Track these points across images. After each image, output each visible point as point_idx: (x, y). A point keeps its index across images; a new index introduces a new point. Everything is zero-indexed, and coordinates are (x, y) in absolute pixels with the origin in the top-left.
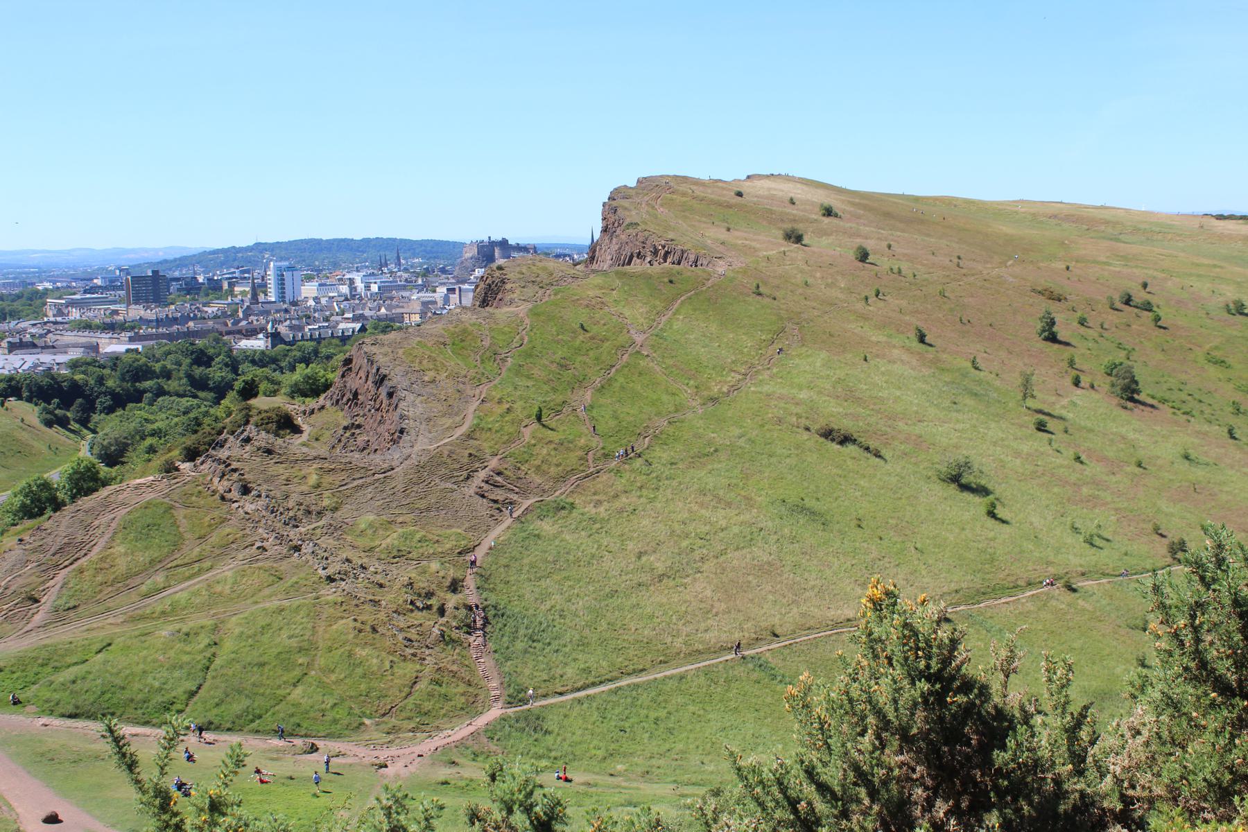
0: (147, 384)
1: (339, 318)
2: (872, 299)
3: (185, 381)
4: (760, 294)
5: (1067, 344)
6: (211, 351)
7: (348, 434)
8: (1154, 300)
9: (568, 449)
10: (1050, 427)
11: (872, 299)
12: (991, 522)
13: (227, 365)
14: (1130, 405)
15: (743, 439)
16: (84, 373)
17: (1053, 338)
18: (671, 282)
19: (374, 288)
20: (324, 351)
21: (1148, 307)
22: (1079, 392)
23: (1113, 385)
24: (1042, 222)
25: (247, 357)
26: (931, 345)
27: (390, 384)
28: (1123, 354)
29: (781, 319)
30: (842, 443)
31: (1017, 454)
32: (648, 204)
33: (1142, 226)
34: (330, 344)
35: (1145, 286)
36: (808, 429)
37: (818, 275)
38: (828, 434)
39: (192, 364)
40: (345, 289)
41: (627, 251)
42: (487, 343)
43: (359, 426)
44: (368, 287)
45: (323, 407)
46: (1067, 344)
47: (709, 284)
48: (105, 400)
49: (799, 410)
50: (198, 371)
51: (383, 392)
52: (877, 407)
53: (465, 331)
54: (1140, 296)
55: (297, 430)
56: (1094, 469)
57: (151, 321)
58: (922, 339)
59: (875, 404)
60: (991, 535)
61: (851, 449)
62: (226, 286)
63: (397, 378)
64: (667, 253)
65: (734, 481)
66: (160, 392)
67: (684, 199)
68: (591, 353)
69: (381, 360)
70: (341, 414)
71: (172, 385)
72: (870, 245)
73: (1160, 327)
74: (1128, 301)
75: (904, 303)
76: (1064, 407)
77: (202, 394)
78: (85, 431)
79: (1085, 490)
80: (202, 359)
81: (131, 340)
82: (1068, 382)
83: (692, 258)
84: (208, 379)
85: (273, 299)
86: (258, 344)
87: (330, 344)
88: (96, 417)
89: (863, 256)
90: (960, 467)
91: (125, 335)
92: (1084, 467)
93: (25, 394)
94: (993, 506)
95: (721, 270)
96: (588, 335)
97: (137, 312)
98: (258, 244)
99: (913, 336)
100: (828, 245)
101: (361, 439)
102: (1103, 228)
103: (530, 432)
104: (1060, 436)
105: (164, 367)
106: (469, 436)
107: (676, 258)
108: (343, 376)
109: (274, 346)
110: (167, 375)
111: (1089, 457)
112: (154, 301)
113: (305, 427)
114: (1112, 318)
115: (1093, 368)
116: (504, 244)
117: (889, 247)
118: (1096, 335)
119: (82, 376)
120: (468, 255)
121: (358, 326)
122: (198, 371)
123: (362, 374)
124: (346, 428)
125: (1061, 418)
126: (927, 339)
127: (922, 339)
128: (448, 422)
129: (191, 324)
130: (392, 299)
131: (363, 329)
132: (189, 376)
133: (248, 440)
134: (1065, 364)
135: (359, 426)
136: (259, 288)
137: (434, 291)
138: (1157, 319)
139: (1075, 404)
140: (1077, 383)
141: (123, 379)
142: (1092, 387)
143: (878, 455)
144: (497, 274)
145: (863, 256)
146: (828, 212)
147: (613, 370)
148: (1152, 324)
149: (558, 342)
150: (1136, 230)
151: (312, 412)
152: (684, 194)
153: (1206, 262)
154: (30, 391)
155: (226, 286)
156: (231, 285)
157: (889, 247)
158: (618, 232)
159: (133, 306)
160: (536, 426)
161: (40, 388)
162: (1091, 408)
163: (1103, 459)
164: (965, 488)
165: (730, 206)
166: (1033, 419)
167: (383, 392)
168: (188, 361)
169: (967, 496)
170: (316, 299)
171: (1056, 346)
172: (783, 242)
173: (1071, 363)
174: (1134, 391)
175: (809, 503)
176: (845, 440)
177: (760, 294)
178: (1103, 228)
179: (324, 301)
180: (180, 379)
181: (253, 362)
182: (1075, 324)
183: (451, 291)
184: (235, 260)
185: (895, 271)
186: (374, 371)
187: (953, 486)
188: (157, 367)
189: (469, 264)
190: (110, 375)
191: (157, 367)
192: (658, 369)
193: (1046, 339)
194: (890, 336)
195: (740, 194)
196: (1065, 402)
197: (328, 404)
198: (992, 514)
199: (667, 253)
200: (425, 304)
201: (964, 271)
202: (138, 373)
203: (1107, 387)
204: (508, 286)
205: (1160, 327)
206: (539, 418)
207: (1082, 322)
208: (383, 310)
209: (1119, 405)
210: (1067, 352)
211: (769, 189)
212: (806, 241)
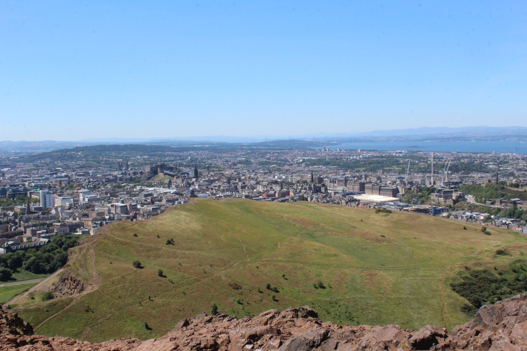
19: (87, 200)
20: (27, 255)
34: (31, 251)
41: (64, 277)
44: (84, 199)
74: (268, 287)
83: (82, 283)
98: (77, 148)
100: (151, 267)
109: (7, 252)
120: (147, 171)
121: (46, 240)
131: (49, 242)
148: (272, 299)
153: (334, 251)
184: (65, 156)
189: (147, 175)
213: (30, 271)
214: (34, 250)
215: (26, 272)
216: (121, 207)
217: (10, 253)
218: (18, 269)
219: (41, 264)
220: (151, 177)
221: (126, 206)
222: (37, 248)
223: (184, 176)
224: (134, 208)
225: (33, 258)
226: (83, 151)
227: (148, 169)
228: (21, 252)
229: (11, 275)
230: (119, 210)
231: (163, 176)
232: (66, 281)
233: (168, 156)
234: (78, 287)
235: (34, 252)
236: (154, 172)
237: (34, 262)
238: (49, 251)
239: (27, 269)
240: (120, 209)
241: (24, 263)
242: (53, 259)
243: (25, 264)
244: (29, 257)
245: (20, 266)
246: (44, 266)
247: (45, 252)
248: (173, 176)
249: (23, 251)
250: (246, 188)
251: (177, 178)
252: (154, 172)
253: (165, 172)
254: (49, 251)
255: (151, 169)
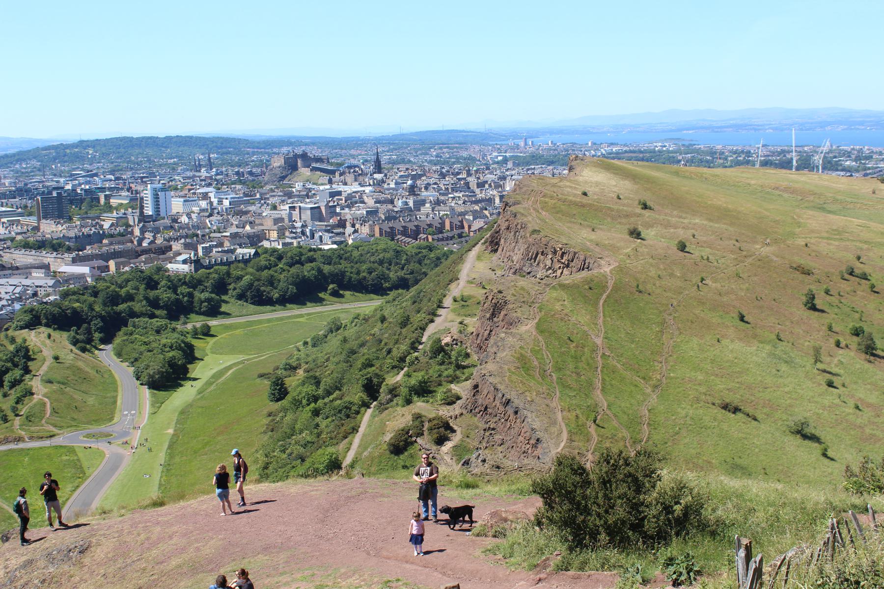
0: (122, 307)
1: (219, 235)
2: (700, 284)
3: (144, 302)
4: (640, 292)
5: (823, 311)
6: (156, 277)
7: (487, 434)
8: (867, 269)
9: (616, 441)
10: (835, 385)
11: (700, 284)
12: (826, 461)
13: (169, 288)
14: (872, 358)
15: (688, 418)
16: (78, 301)
17: (814, 308)
18: (590, 288)
19: (226, 203)
20: (235, 273)
21: (864, 277)
22: (841, 351)
23: (859, 345)
24: (768, 193)
25: (180, 280)
26: (747, 322)
27: (514, 405)
28: (857, 316)
29: (660, 312)
30: (734, 413)
31: (824, 408)
32: (534, 209)
33: (839, 197)
34: (238, 267)
35: (859, 258)
36: (714, 404)
37: (662, 267)
38: (725, 407)
39: (146, 289)
40: (204, 204)
41: (534, 250)
42: (536, 363)
43: (493, 429)
44: (220, 202)
45: (462, 414)
46: (823, 311)
47: (610, 284)
48: (97, 323)
49: (703, 389)
50: (152, 294)
51: (510, 411)
52: (739, 380)
53: (521, 355)
54: (859, 268)
55: (454, 431)
56: (867, 413)
57: (71, 238)
58: (742, 318)
59: (737, 378)
60: (830, 470)
61: (740, 415)
62: (102, 201)
63: (517, 402)
64: (563, 254)
65: (698, 450)
66: (133, 314)
67: (553, 202)
68: (583, 359)
69: (501, 387)
70: (476, 419)
71: (137, 307)
72: (682, 234)
73: (875, 292)
75: (718, 285)
76: (836, 366)
77: (158, 312)
78: (93, 349)
79: (868, 431)
80: (152, 284)
81: (74, 261)
82: (832, 341)
83: (582, 258)
84: (160, 300)
85: (151, 213)
86: (178, 267)
87: (238, 267)
88: (97, 335)
89: (682, 247)
90: (803, 424)
91: (69, 257)
92: (860, 413)
93: (44, 321)
94: (826, 450)
95: (607, 269)
96: (574, 345)
97: (50, 228)
98: (82, 142)
99: (736, 316)
101: (498, 437)
102: (812, 198)
103: (592, 429)
104: (842, 389)
105: (128, 292)
106: (571, 440)
107: (570, 257)
108: (474, 395)
109: (196, 270)
110: (130, 298)
111: (862, 405)
112: (60, 216)
113: (455, 427)
114: (845, 286)
115: (843, 327)
116: (304, 156)
117: (694, 236)
118: (837, 301)
119: (78, 304)
120: (276, 165)
121: (253, 251)
122: (152, 294)
123: (491, 396)
124: (485, 430)
125: (838, 375)
126: (745, 319)
127: (742, 318)
128: (554, 430)
129: (105, 241)
130: (246, 213)
131: (257, 254)
132: (146, 298)
133: (484, 461)
134: (825, 328)
135: (493, 429)
136: (137, 202)
137: (274, 208)
138: (873, 286)
139: (842, 363)
140: (838, 344)
141: (105, 304)
142: (847, 346)
143: (755, 419)
144: (500, 296)
145: (682, 247)
146: (645, 207)
147: (599, 370)
148: (869, 290)
149: (563, 353)
150: (835, 201)
151: (456, 417)
152: (552, 197)
154: (47, 318)
155: (102, 201)
156: (107, 198)
157: (694, 236)
158: (522, 233)
159: (43, 221)
160: (593, 425)
161: (54, 315)
162: (848, 360)
163: (869, 405)
164: (805, 437)
165: (583, 206)
166: (823, 379)
167: (510, 411)
168: (143, 286)
169: (807, 442)
170: (189, 215)
171: (817, 313)
172: (628, 237)
173: (830, 328)
174: (873, 349)
175: (738, 461)
176: (736, 410)
177: (640, 292)
178: (812, 198)
179: (194, 216)
180: (142, 301)
181: (185, 283)
182: (823, 293)
183: (292, 208)
184: (65, 155)
185: (705, 257)
186: (500, 395)
187: (798, 436)
188: (123, 292)
189: (278, 171)
190: (95, 302)
191: (123, 292)
192: (619, 366)
193: (810, 308)
194: (721, 317)
195: (585, 194)
196: (836, 360)
197: (465, 412)
198: (825, 455)
199: (563, 254)
200: (277, 221)
201: (745, 253)
202: (114, 299)
203: (854, 346)
204: (510, 306)
205: (875, 292)
206: (595, 421)
207: (827, 292)
208: (248, 228)
209: (866, 360)
210: (826, 319)
211: (597, 184)
212: (643, 236)
213: (247, 301)
214: (241, 265)
215: (240, 302)
216: (312, 208)
217: (202, 271)
218: (224, 297)
219: (262, 288)
220: (286, 176)
221: (319, 207)
222: (246, 262)
223: (354, 171)
224: (331, 210)
225: (247, 278)
226: (94, 147)
227: (278, 162)
228: (224, 268)
229: (220, 307)
230: (307, 215)
231: (309, 173)
232: (540, 257)
233: (254, 154)
234: (572, 264)
235: (243, 269)
236: (291, 166)
237: (250, 285)
238: (266, 268)
239: (241, 297)
240: (309, 212)
241: (231, 287)
242: (279, 281)
243: (235, 289)
244: (239, 278)
245: (226, 293)
246: (269, 293)
247: (261, 269)
248: (333, 172)
249: (226, 268)
250: (487, 186)
251: (341, 175)
252: (291, 166)
253: (314, 165)
254: (266, 268)
255: (287, 160)
